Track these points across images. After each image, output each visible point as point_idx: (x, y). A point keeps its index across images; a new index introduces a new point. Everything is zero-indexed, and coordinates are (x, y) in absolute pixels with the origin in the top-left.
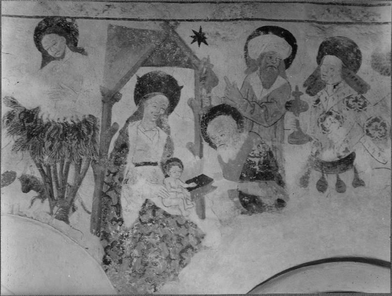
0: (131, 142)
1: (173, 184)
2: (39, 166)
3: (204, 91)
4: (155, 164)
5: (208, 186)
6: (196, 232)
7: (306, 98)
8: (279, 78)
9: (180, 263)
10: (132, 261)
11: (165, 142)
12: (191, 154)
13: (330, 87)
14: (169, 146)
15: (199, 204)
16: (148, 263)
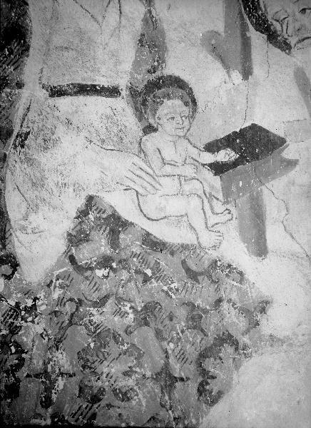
1: (169, 153)
4: (113, 92)
5: (270, 161)
6: (243, 294)
9: (201, 390)
10: (48, 390)
11: (139, 25)
12: (218, 65)
15: (247, 212)
16: (102, 391)
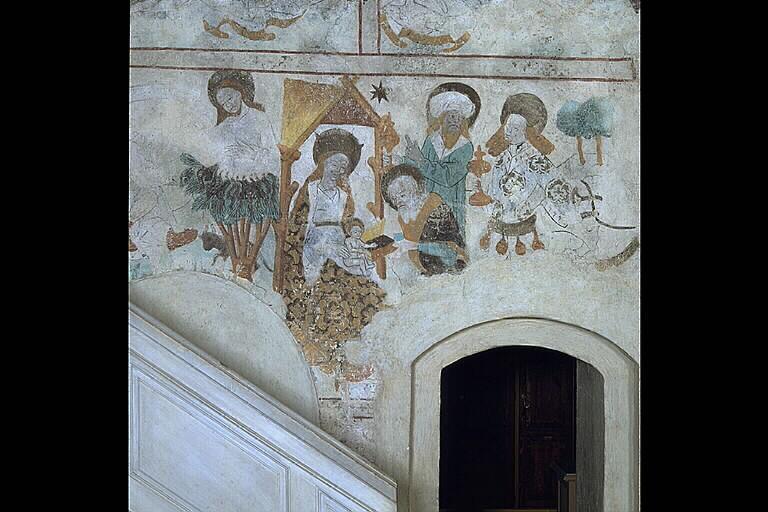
0: (312, 200)
2: (220, 224)
3: (385, 150)
7: (488, 158)
8: (462, 137)
13: (514, 147)
14: (349, 206)
